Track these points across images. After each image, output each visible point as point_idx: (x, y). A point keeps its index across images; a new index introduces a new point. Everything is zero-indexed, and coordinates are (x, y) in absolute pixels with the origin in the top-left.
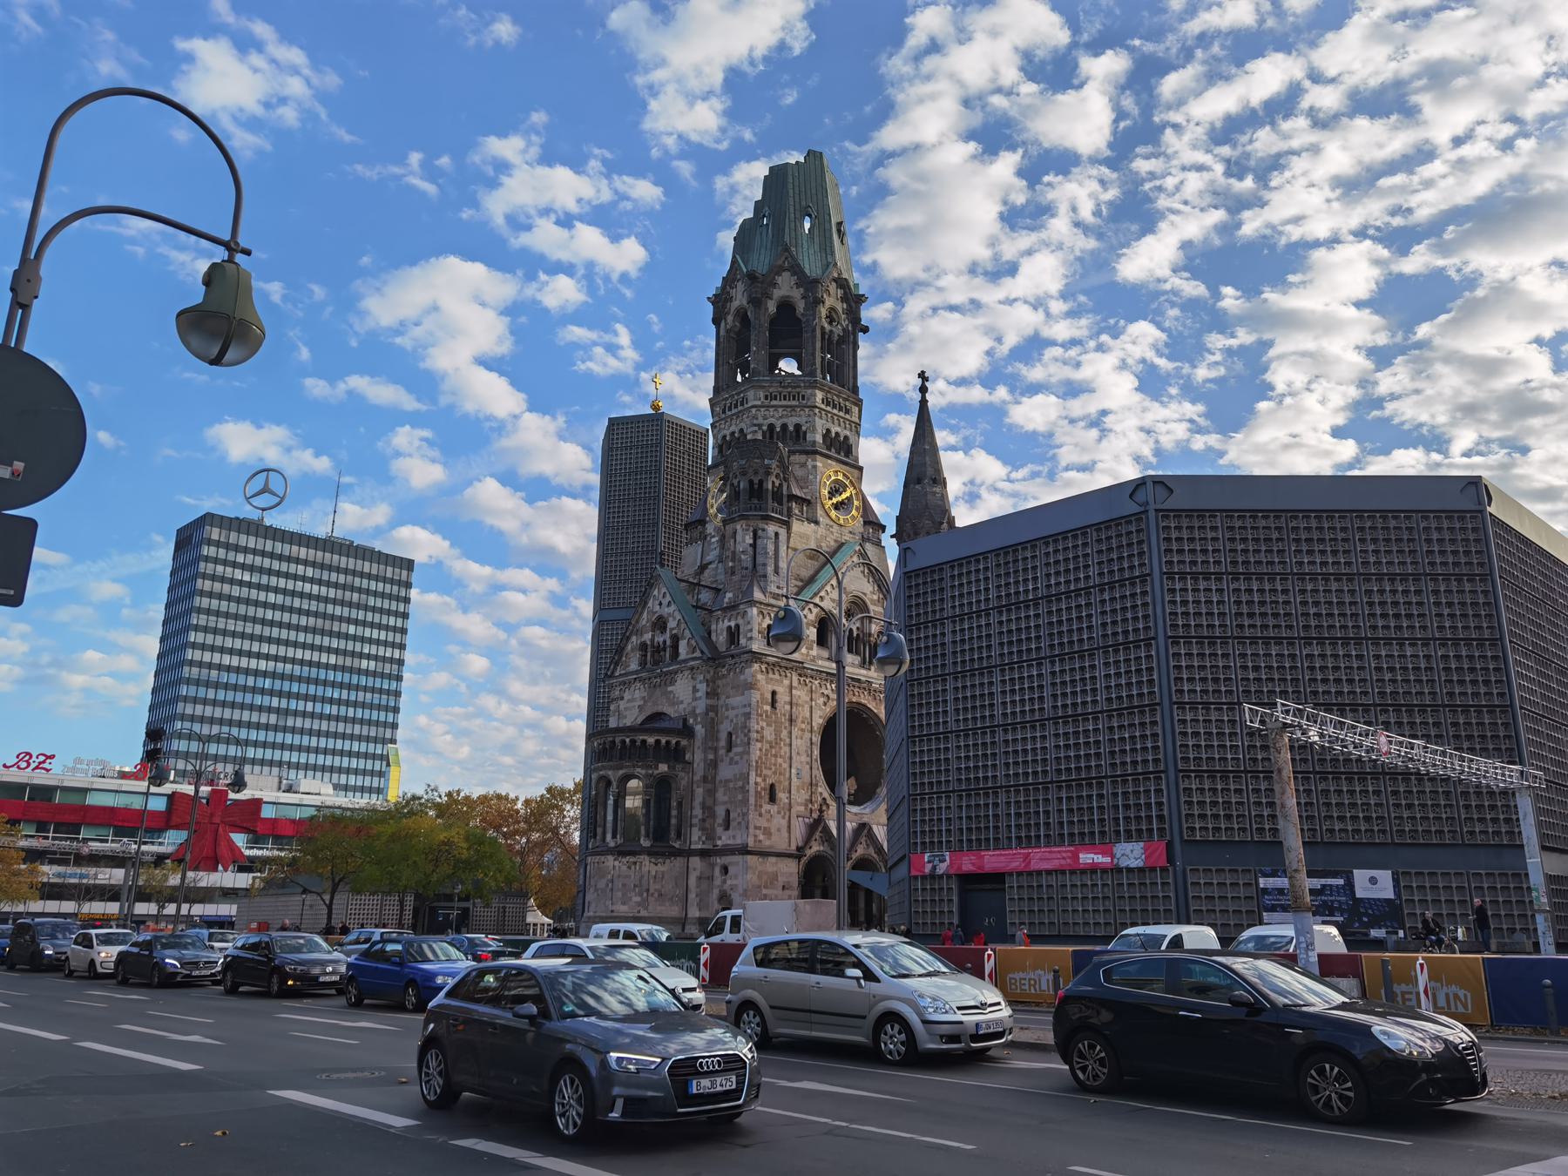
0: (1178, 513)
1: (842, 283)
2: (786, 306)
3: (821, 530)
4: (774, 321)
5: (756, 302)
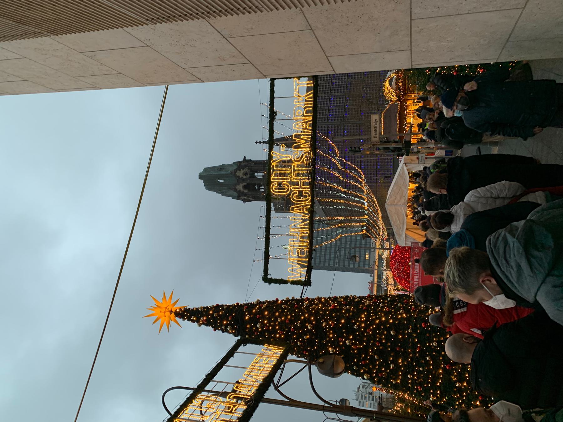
1: (236, 170)
2: (245, 187)
4: (249, 190)
5: (245, 195)
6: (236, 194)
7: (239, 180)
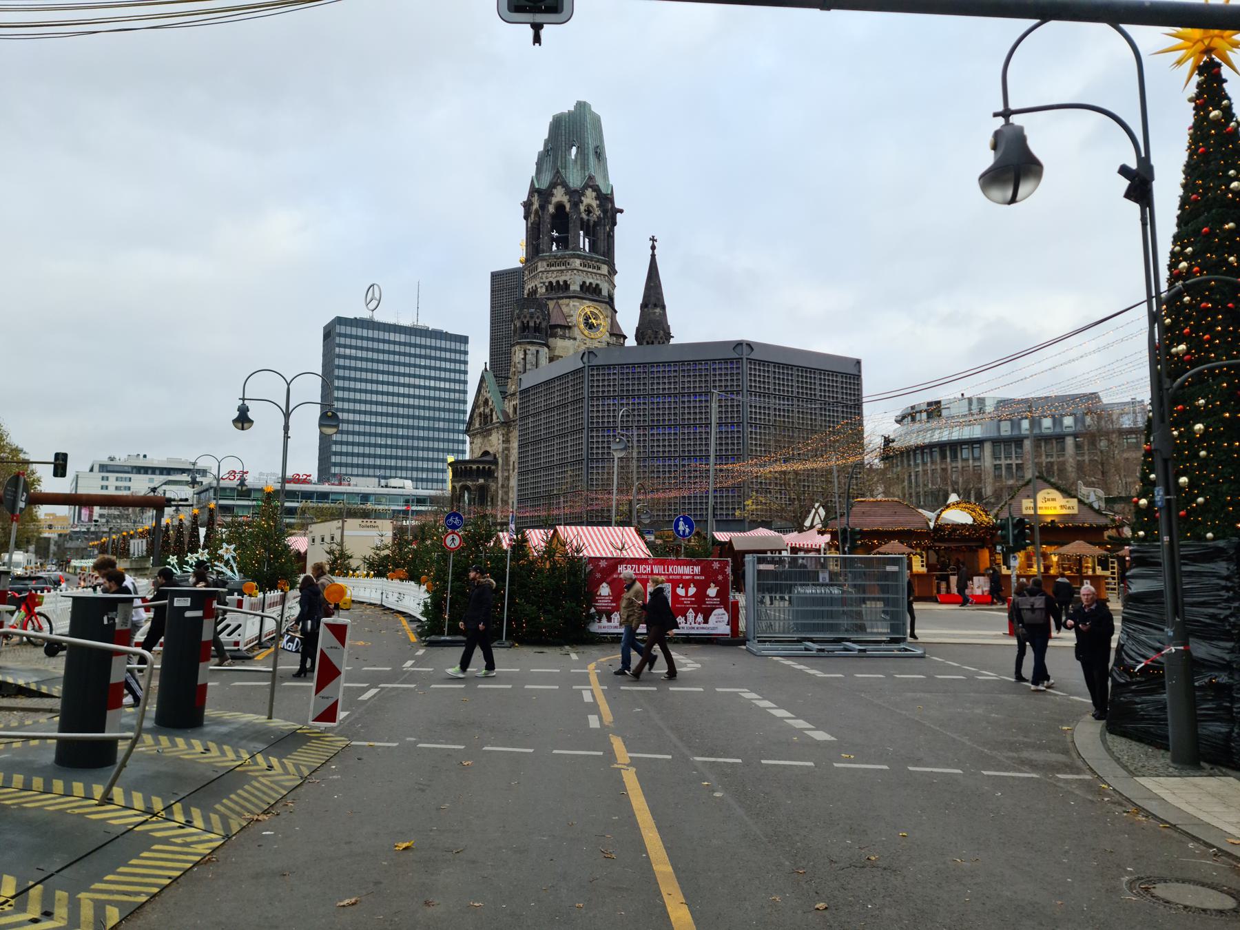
0: (598, 367)
1: (596, 189)
2: (560, 207)
3: (577, 343)
4: (553, 216)
5: (543, 207)
6: (544, 184)
7: (576, 195)
